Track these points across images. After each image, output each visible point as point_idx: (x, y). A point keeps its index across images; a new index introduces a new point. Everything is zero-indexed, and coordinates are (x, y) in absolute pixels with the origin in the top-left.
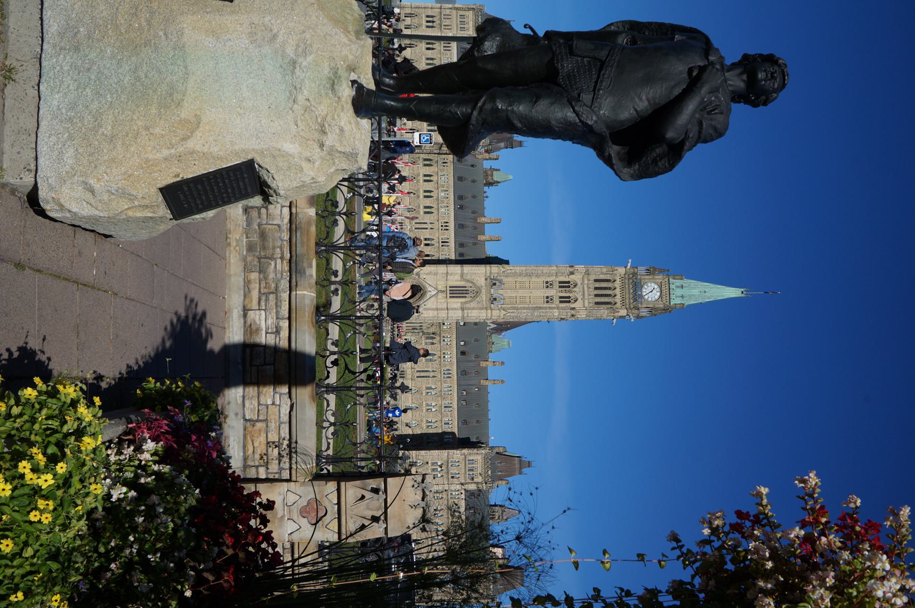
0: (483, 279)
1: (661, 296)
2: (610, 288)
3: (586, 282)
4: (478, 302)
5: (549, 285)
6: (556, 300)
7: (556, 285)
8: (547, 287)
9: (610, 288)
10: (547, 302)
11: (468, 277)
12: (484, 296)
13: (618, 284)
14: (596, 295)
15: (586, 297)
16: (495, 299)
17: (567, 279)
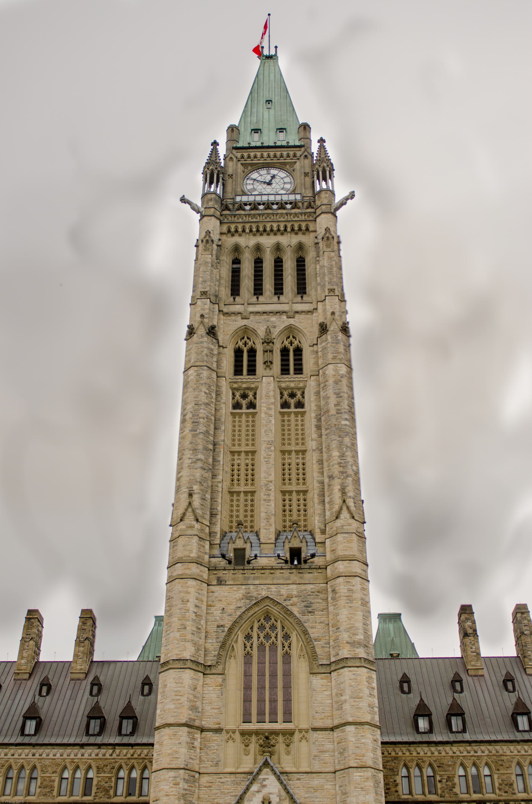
0: (220, 591)
1: (281, 167)
2: (258, 263)
3: (238, 308)
4: (309, 609)
5: (245, 402)
6: (292, 381)
7: (245, 379)
8: (252, 405)
9: (258, 263)
10: (300, 405)
11: (213, 645)
12: (287, 588)
13: (247, 242)
14: (279, 290)
15: (285, 307)
16: (295, 553)
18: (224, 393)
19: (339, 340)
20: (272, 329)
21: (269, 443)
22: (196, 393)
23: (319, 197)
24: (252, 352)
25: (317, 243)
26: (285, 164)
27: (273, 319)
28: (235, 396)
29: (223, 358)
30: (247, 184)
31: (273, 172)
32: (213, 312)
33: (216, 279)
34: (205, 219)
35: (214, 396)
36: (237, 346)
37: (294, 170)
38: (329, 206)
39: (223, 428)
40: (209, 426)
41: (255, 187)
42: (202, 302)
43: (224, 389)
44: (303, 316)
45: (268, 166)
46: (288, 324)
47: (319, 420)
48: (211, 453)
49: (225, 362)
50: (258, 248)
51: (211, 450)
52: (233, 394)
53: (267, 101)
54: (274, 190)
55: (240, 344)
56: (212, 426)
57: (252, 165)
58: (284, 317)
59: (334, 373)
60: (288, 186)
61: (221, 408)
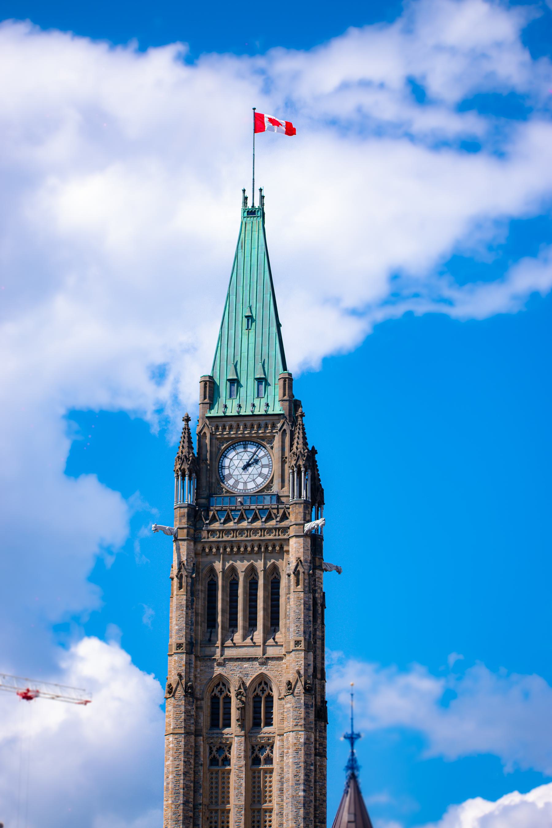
15: (258, 652)
17: (206, 704)
18: (202, 753)
19: (300, 703)
20: (244, 679)
21: (239, 807)
22: (177, 763)
23: (293, 508)
24: (228, 699)
25: (289, 575)
26: (263, 439)
27: (246, 665)
28: (212, 751)
29: (201, 714)
30: (222, 467)
31: (252, 449)
32: (190, 664)
33: (192, 621)
34: (180, 542)
35: (192, 761)
36: (213, 694)
37: (272, 448)
38: (302, 526)
39: (201, 791)
40: (188, 794)
41: (231, 471)
42: (179, 657)
43: (202, 750)
44: (274, 662)
45: (245, 442)
46: (260, 672)
47: (282, 783)
48: (192, 820)
49: (202, 718)
50: (233, 569)
51: (191, 817)
52: (211, 748)
53: (246, 317)
54: (251, 476)
55: (216, 691)
56: (192, 793)
57: (227, 440)
58: (256, 664)
59: (295, 741)
60: (265, 471)
61: (199, 771)
